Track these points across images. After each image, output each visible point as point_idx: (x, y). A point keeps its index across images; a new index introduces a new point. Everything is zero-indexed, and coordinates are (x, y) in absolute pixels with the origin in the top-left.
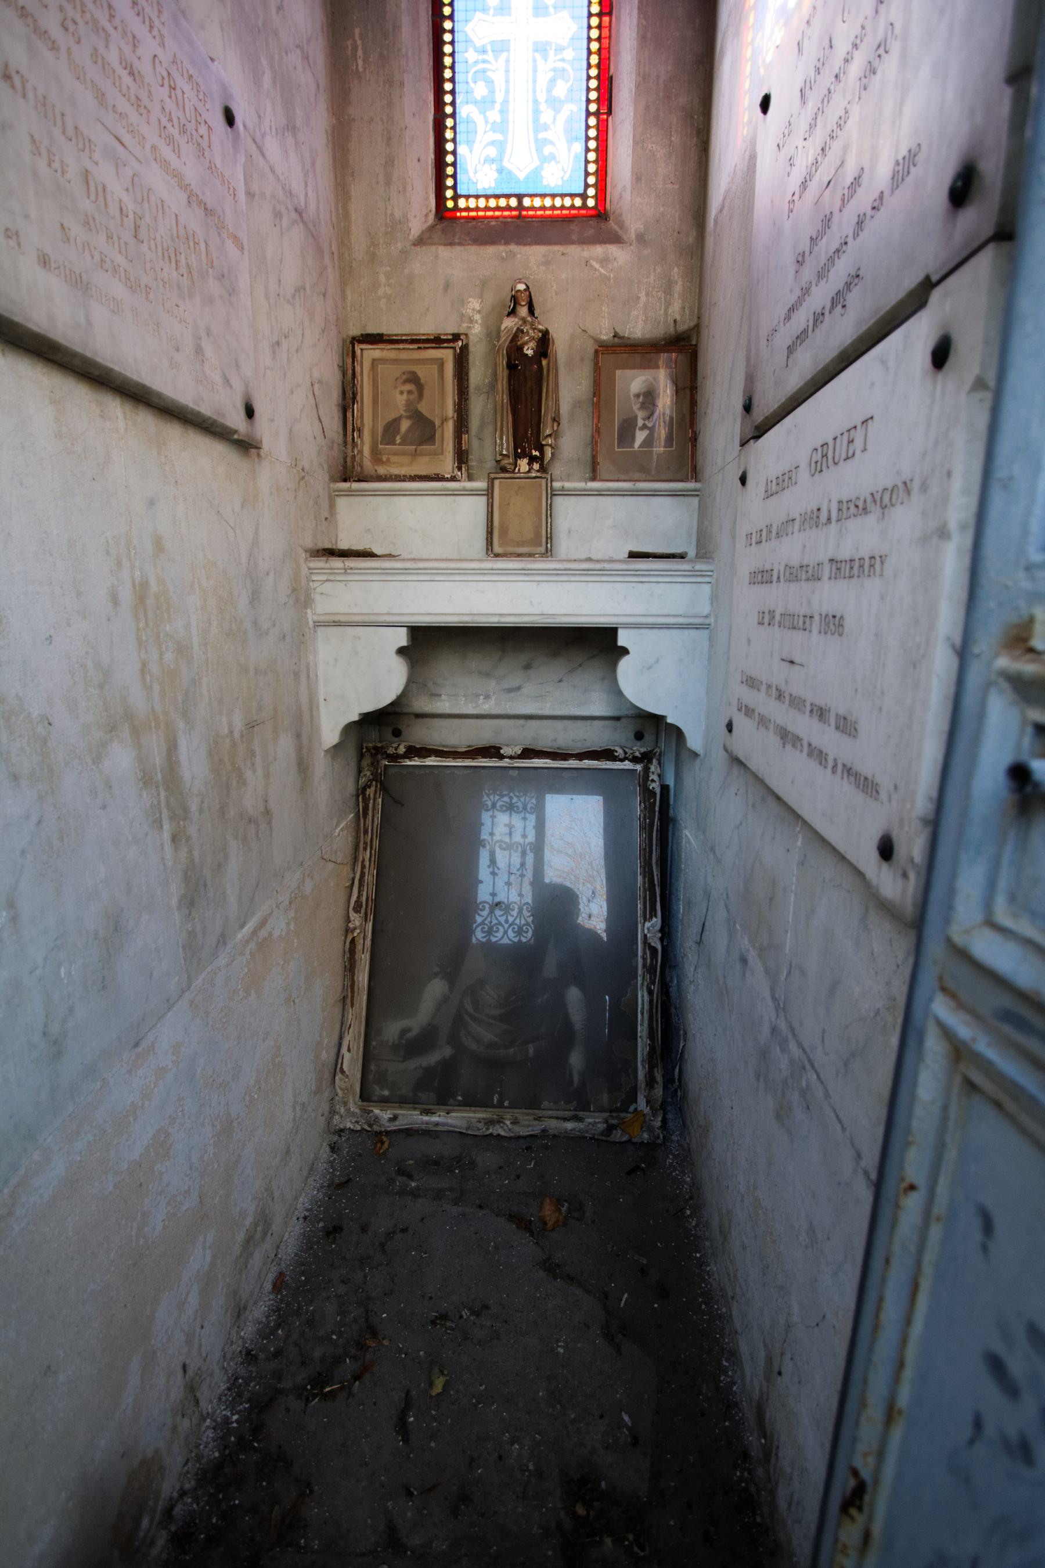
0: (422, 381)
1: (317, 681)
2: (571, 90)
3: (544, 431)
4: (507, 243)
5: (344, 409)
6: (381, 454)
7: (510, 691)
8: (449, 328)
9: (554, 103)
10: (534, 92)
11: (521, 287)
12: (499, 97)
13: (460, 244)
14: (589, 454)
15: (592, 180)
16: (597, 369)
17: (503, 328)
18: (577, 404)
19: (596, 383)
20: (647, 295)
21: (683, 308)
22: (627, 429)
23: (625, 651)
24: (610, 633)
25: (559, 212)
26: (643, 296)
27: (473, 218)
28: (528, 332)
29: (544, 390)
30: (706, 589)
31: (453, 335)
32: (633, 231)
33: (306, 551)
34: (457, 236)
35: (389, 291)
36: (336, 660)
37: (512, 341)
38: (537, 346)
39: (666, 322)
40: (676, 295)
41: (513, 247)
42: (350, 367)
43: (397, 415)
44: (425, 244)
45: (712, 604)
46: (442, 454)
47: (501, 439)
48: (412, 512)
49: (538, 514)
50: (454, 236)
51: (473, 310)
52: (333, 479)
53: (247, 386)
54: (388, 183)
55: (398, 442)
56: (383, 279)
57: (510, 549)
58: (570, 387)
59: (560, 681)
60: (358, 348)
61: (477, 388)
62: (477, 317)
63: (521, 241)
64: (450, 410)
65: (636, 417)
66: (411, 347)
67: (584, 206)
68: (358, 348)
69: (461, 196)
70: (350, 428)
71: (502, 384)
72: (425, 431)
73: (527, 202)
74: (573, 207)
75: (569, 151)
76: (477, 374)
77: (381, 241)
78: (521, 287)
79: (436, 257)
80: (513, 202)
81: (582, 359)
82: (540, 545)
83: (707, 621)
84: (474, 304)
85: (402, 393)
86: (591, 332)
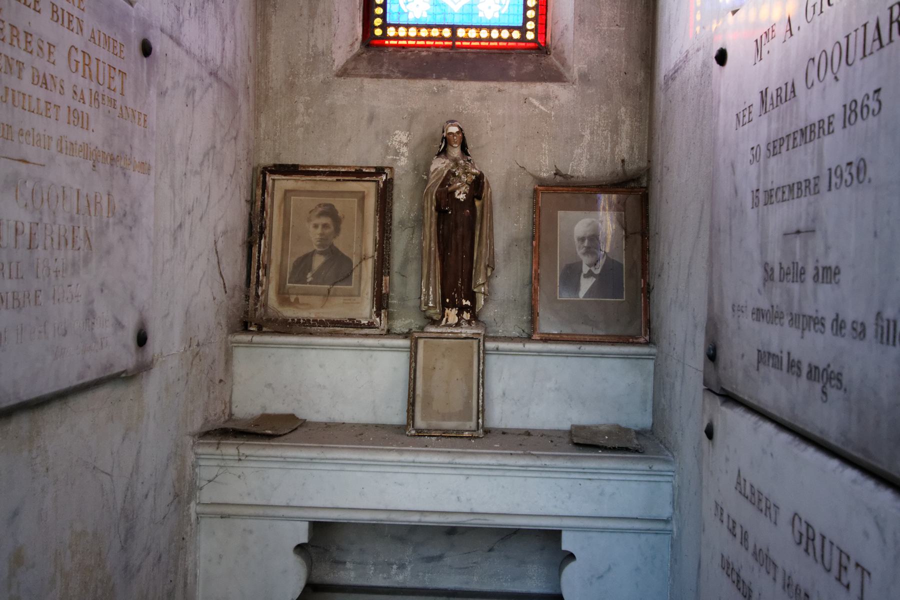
0: (340, 214)
1: (195, 583)
3: (477, 279)
4: (439, 77)
5: (250, 244)
6: (288, 293)
7: (430, 559)
8: (373, 160)
11: (454, 129)
13: (388, 77)
14: (527, 296)
15: (531, 14)
16: (536, 208)
17: (432, 169)
18: (514, 242)
19: (536, 224)
20: (592, 133)
21: (632, 148)
22: (572, 274)
24: (554, 535)
25: (496, 44)
26: (587, 137)
27: (403, 46)
28: (459, 177)
29: (477, 233)
30: (667, 489)
32: (576, 70)
33: (194, 436)
34: (385, 67)
35: (307, 120)
36: (221, 557)
37: (442, 185)
38: (470, 190)
39: (612, 161)
40: (624, 135)
41: (445, 82)
42: (259, 198)
43: (310, 250)
44: (349, 75)
46: (359, 295)
47: (428, 289)
48: (321, 366)
49: (468, 375)
50: (381, 67)
51: (400, 142)
52: (233, 331)
53: (141, 313)
54: (312, 15)
55: (309, 280)
56: (301, 108)
57: (435, 423)
58: (506, 225)
59: (490, 550)
60: (269, 178)
61: (401, 222)
62: (404, 150)
63: (454, 76)
64: (370, 247)
65: (581, 263)
66: (329, 179)
67: (523, 38)
68: (269, 178)
69: (390, 25)
70: (255, 265)
72: (340, 269)
73: (461, 33)
74: (510, 39)
76: (401, 208)
77: (302, 71)
78: (454, 129)
79: (361, 89)
80: (447, 33)
81: (520, 196)
82: (470, 420)
83: (669, 527)
84: (402, 136)
85: (316, 226)
86: (530, 168)
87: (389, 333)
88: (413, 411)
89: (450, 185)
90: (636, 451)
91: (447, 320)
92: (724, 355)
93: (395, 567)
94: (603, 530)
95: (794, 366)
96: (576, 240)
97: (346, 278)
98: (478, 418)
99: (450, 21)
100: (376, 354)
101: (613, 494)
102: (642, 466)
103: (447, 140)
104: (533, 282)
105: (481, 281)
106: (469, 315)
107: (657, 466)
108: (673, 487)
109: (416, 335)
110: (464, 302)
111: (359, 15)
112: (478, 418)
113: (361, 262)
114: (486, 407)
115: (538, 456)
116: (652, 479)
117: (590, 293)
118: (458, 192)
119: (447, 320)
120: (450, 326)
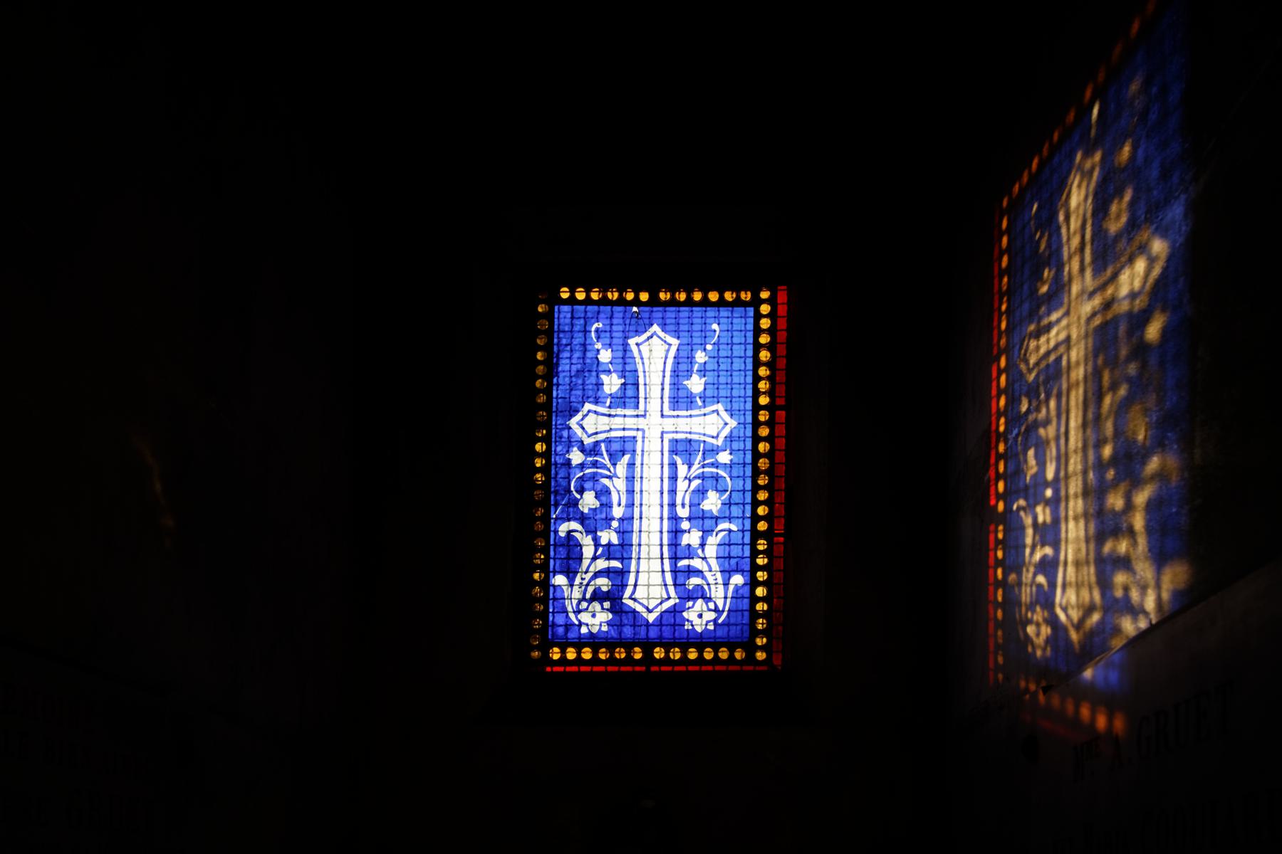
2: (728, 504)
9: (702, 519)
10: (672, 505)
12: (618, 512)
73: (659, 653)
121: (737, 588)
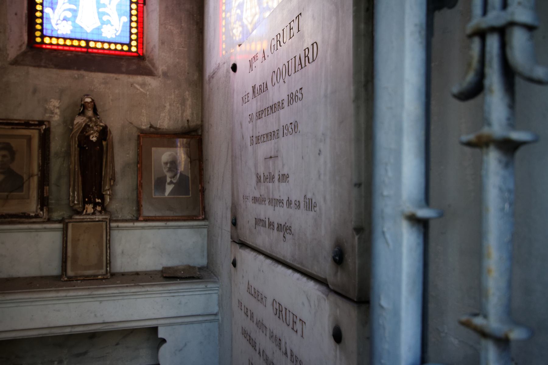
4: (79, 69)
7: (78, 355)
8: (37, 117)
14: (135, 196)
16: (139, 146)
17: (75, 122)
19: (139, 155)
20: (170, 105)
21: (193, 114)
22: (161, 183)
23: (164, 341)
24: (154, 330)
26: (168, 107)
27: (55, 50)
28: (92, 127)
29: (104, 160)
30: (215, 297)
31: (38, 121)
38: (99, 135)
40: (188, 106)
41: (82, 72)
45: (219, 307)
46: (29, 198)
47: (74, 193)
51: (54, 106)
58: (122, 156)
59: (117, 344)
64: (35, 169)
65: (165, 177)
66: (7, 127)
69: (46, 36)
71: (75, 157)
75: (120, 20)
76: (56, 145)
78: (88, 100)
80: (83, 44)
82: (102, 268)
83: (217, 318)
84: (56, 103)
87: (49, 220)
88: (66, 266)
89: (87, 132)
90: (198, 278)
91: (86, 211)
92: (240, 222)
93: (56, 363)
94: (181, 324)
95: (271, 224)
96: (163, 164)
97: (20, 188)
98: (107, 267)
99: (84, 37)
100: (40, 234)
101: (186, 303)
102: (202, 286)
103: (84, 106)
104: (139, 188)
105: (107, 188)
106: (100, 208)
107: (210, 285)
108: (219, 295)
109: (67, 221)
110: (97, 200)
111: (25, 29)
112: (107, 267)
113: (29, 178)
114: (112, 260)
115: (143, 286)
116: (207, 292)
117: (172, 193)
118: (91, 136)
119: (86, 211)
120: (89, 214)
121: (124, 23)
